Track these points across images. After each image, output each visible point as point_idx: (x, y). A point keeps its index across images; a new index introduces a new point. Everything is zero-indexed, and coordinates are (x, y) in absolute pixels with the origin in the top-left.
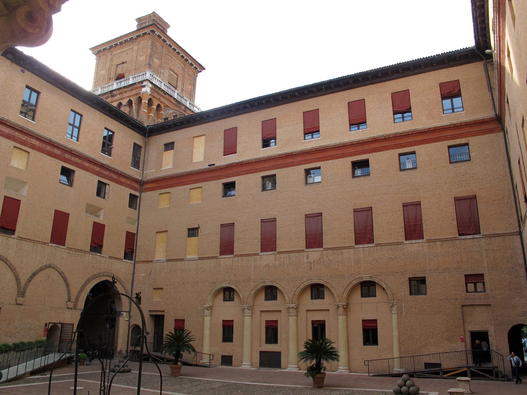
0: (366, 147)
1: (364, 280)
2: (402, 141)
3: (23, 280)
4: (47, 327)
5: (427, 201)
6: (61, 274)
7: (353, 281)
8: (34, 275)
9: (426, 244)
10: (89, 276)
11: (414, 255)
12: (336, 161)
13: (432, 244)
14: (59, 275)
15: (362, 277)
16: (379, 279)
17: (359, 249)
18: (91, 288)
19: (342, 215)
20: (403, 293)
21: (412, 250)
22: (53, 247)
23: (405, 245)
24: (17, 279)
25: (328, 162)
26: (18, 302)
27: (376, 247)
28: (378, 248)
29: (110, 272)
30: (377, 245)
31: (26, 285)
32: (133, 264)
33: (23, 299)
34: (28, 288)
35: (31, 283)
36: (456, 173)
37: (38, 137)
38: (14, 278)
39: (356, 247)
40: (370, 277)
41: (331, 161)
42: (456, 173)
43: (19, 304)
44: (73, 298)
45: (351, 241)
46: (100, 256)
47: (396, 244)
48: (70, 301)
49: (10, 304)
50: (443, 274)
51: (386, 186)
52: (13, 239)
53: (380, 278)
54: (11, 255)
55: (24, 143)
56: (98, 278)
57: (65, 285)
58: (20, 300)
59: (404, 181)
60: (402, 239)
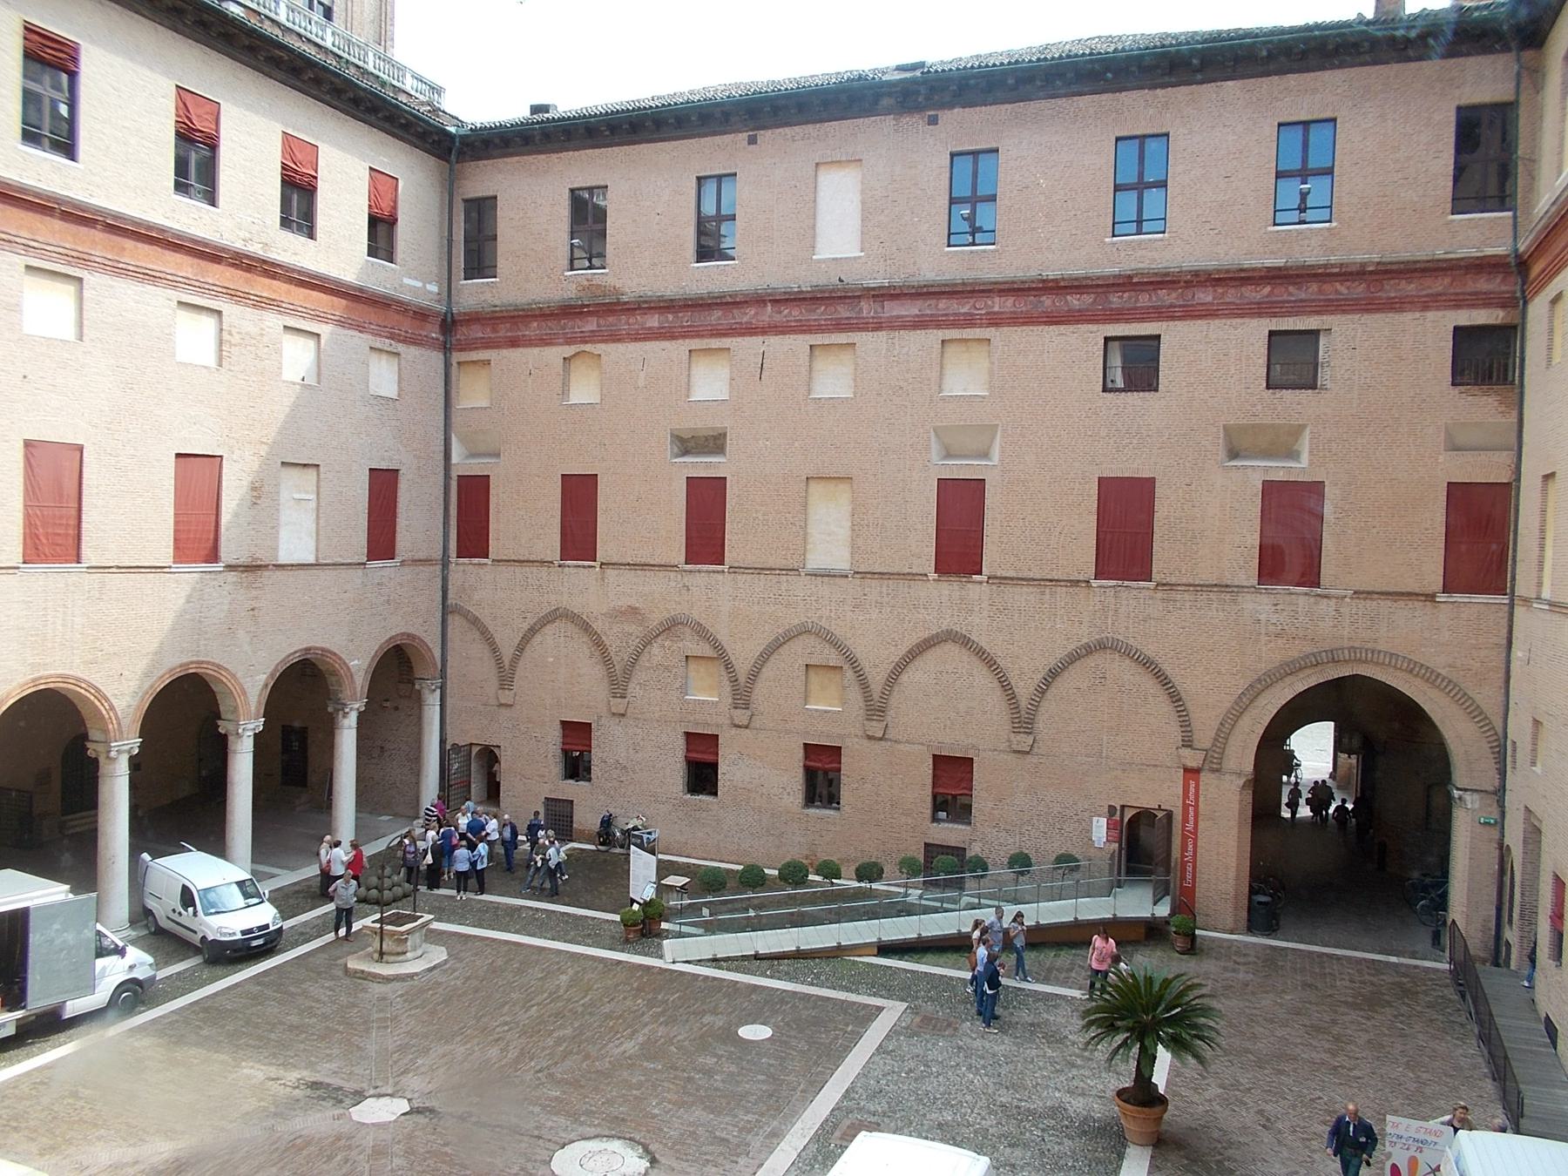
6: (1148, 664)
8: (1053, 674)
10: (1263, 667)
14: (1141, 670)
22: (1107, 590)
26: (1015, 747)
29: (1369, 646)
31: (1035, 705)
32: (1506, 608)
33: (1030, 740)
37: (1002, 287)
46: (1306, 594)
52: (977, 587)
54: (979, 627)
55: (969, 322)
56: (1308, 672)
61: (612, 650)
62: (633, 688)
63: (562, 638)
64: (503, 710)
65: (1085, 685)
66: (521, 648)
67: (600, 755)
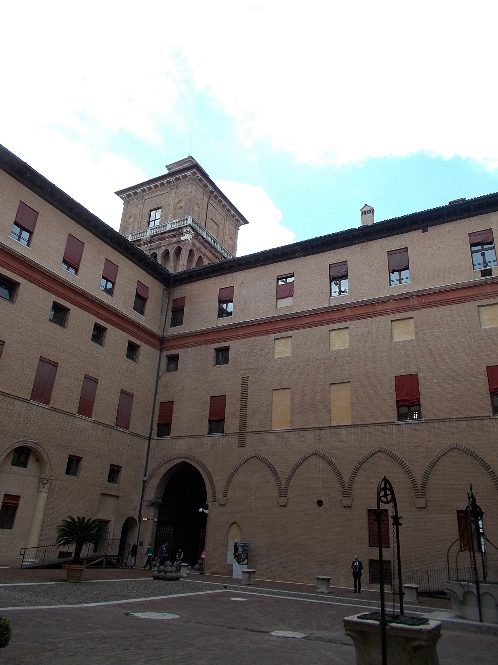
0: (72, 295)
1: (28, 445)
2: (101, 312)
5: (103, 382)
7: (16, 443)
9: (92, 425)
11: (80, 432)
12: (40, 289)
13: (96, 426)
15: (27, 441)
16: (43, 449)
17: (34, 406)
19: (26, 357)
20: (60, 470)
21: (80, 426)
23: (76, 418)
25: (31, 284)
27: (49, 411)
28: (52, 412)
30: (52, 409)
36: (127, 368)
39: (31, 402)
40: (35, 443)
41: (34, 285)
42: (127, 368)
45: (27, 394)
47: (69, 414)
50: (96, 458)
51: (77, 348)
53: (44, 447)
59: (92, 353)
60: (75, 411)
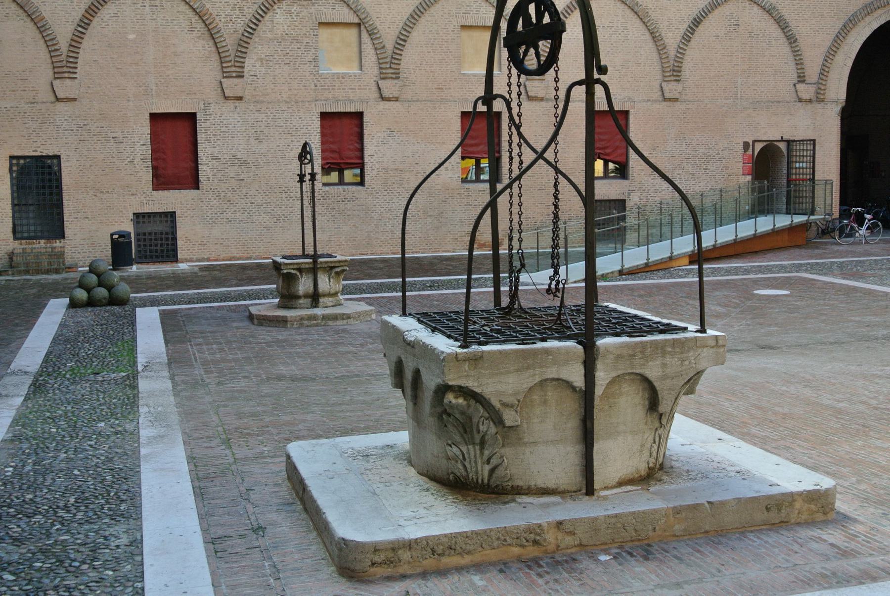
3: (672, 39)
4: (750, 152)
8: (697, 22)
14: (766, 16)
18: (862, 42)
24: (655, 37)
26: (667, 95)
31: (681, 51)
33: (679, 87)
34: (686, 57)
35: (693, 43)
38: (648, 36)
43: (670, 100)
44: (812, 72)
48: (803, 81)
49: (649, 100)
56: (879, 12)
57: (785, 40)
58: (671, 89)
61: (221, 22)
62: (250, 64)
63: (147, 8)
64: (60, 106)
65: (723, 33)
66: (85, 23)
67: (210, 150)
